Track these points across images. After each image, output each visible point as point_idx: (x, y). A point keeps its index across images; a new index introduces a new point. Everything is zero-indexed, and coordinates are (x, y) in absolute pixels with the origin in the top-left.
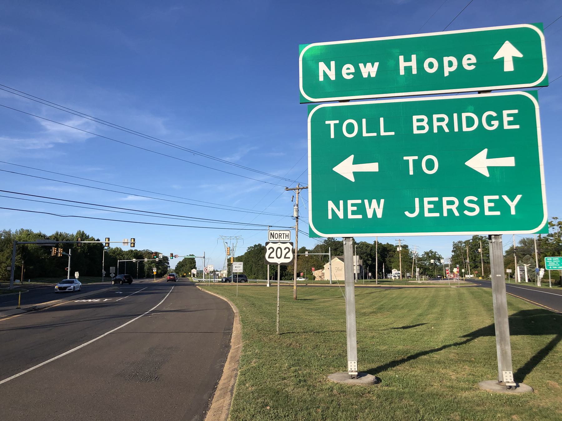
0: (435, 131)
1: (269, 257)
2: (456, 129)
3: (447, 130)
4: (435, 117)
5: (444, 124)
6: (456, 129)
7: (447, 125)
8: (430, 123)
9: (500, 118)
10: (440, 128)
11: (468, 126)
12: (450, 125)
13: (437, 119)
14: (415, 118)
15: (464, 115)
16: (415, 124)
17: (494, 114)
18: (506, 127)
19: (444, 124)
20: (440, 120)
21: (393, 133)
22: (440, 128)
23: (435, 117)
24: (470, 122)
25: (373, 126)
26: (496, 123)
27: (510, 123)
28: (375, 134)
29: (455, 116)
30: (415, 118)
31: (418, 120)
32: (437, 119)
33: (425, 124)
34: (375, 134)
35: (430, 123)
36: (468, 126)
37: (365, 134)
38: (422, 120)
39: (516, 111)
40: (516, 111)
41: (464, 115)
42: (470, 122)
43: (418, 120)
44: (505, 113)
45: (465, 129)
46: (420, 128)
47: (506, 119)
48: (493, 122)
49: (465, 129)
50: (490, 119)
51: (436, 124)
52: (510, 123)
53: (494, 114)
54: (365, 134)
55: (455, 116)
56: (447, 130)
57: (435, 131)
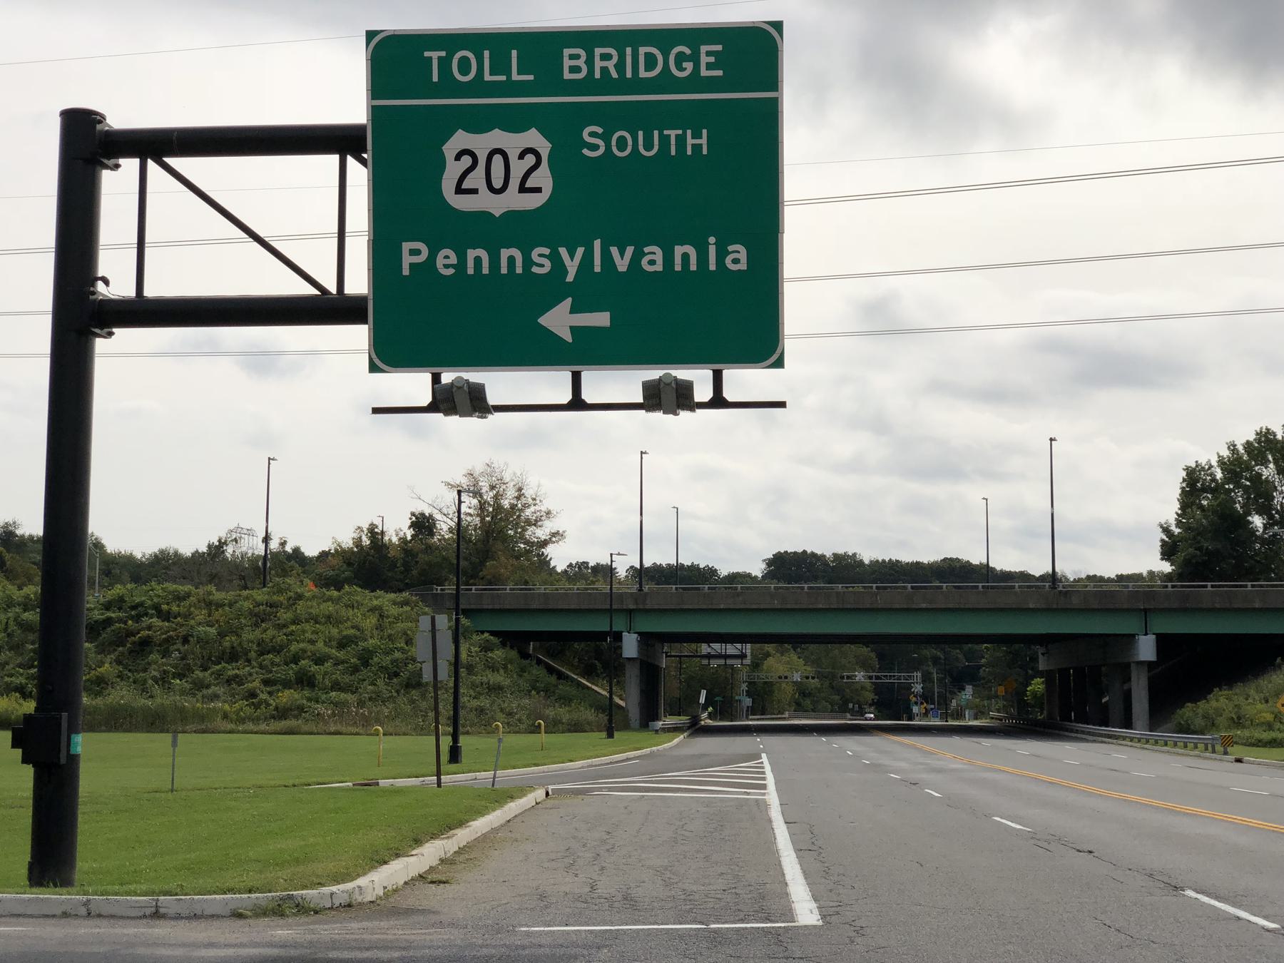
0: (597, 75)
1: (459, 190)
2: (629, 75)
3: (615, 75)
4: (598, 51)
5: (610, 65)
6: (629, 75)
8: (590, 62)
9: (695, 58)
10: (604, 70)
12: (620, 66)
14: (567, 52)
15: (643, 50)
16: (567, 63)
17: (688, 51)
18: (704, 72)
19: (610, 65)
20: (606, 57)
21: (531, 77)
22: (604, 70)
23: (598, 51)
25: (500, 65)
26: (689, 66)
27: (709, 66)
28: (503, 78)
29: (629, 50)
30: (567, 52)
31: (572, 57)
33: (581, 62)
34: (503, 78)
35: (590, 62)
37: (487, 77)
38: (577, 57)
39: (719, 48)
40: (719, 48)
41: (643, 50)
43: (572, 57)
44: (704, 49)
45: (643, 74)
47: (704, 60)
48: (685, 65)
50: (680, 58)
51: (598, 64)
52: (709, 66)
53: (688, 51)
54: (487, 77)
55: (629, 50)
56: (615, 75)
57: (597, 75)
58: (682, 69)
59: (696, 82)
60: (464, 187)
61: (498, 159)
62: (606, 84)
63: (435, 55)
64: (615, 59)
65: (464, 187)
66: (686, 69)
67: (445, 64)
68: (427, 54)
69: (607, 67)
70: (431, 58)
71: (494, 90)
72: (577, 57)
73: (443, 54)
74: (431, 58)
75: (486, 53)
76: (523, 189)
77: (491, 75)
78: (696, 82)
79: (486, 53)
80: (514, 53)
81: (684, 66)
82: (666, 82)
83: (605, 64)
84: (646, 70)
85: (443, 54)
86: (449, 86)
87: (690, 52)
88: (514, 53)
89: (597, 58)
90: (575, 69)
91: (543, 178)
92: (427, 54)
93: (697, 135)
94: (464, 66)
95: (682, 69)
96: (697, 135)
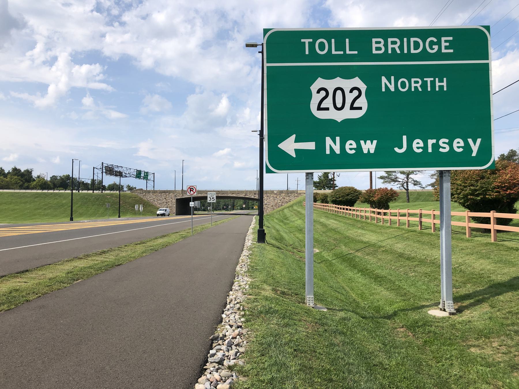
0: (390, 52)
2: (406, 51)
4: (390, 40)
5: (396, 47)
6: (406, 52)
8: (386, 45)
9: (439, 43)
10: (393, 49)
12: (401, 47)
14: (374, 40)
15: (412, 40)
16: (374, 46)
17: (435, 40)
18: (444, 51)
19: (396, 47)
20: (394, 43)
21: (356, 52)
22: (393, 49)
23: (390, 40)
25: (340, 46)
26: (436, 47)
27: (446, 48)
28: (342, 53)
30: (374, 40)
31: (377, 43)
33: (381, 45)
34: (342, 53)
35: (386, 45)
37: (334, 52)
38: (379, 43)
39: (451, 38)
40: (451, 38)
41: (412, 40)
43: (377, 43)
44: (443, 39)
45: (413, 51)
46: (378, 49)
47: (444, 44)
48: (434, 47)
49: (413, 51)
50: (432, 43)
51: (390, 46)
52: (446, 48)
53: (435, 40)
54: (334, 52)
57: (390, 52)
58: (432, 49)
59: (439, 55)
61: (339, 93)
62: (394, 56)
63: (307, 41)
64: (399, 44)
66: (434, 49)
67: (312, 45)
68: (303, 40)
70: (305, 43)
72: (379, 43)
73: (311, 40)
74: (305, 43)
75: (333, 40)
76: (352, 108)
78: (439, 55)
79: (333, 40)
80: (347, 40)
82: (424, 55)
83: (393, 46)
84: (414, 49)
85: (311, 40)
86: (314, 56)
87: (437, 41)
88: (347, 40)
89: (389, 43)
90: (378, 49)
91: (362, 102)
92: (303, 40)
94: (322, 46)
95: (432, 49)
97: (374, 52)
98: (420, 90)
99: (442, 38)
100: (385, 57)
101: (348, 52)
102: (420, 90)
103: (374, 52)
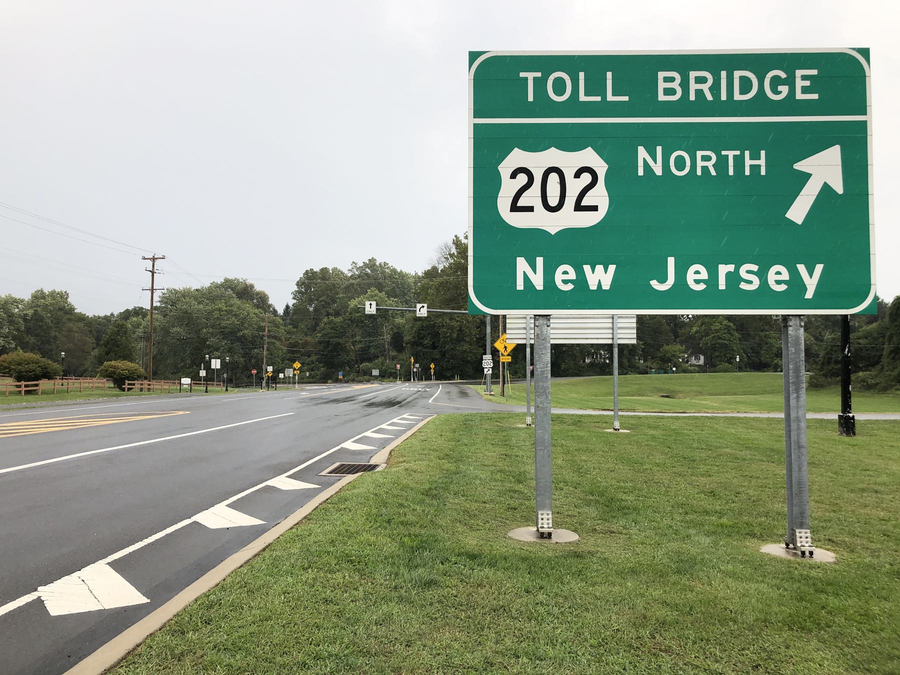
0: (692, 97)
1: (515, 208)
2: (724, 97)
3: (709, 97)
4: (693, 75)
5: (705, 87)
6: (724, 97)
7: (709, 88)
8: (685, 85)
9: (790, 82)
10: (699, 93)
11: (743, 92)
12: (715, 89)
13: (696, 78)
14: (661, 75)
15: (737, 74)
16: (662, 85)
17: (783, 75)
18: (799, 96)
19: (705, 87)
20: (700, 80)
21: (626, 98)
22: (699, 93)
23: (693, 75)
24: (746, 85)
27: (805, 90)
28: (598, 99)
29: (724, 74)
30: (661, 75)
31: (667, 80)
32: (696, 78)
33: (676, 85)
34: (598, 99)
35: (685, 85)
36: (743, 92)
37: (583, 98)
38: (672, 80)
39: (814, 72)
40: (814, 72)
41: (737, 74)
42: (746, 85)
43: (667, 80)
44: (799, 73)
45: (737, 97)
46: (671, 92)
47: (800, 84)
48: (780, 88)
49: (737, 97)
50: (776, 82)
51: (693, 87)
52: (805, 90)
53: (783, 75)
54: (583, 98)
55: (724, 74)
56: (709, 97)
57: (692, 97)
60: (583, 203)
61: (554, 178)
62: (701, 106)
63: (530, 76)
65: (583, 203)
67: (540, 84)
68: (522, 75)
69: (702, 90)
70: (526, 79)
71: (717, 108)
72: (672, 80)
73: (539, 75)
74: (526, 79)
75: (582, 75)
77: (613, 95)
78: (791, 106)
79: (582, 75)
80: (609, 75)
81: (779, 90)
82: (761, 105)
83: (700, 86)
85: (539, 75)
86: (544, 106)
87: (786, 76)
90: (669, 92)
92: (522, 75)
93: (755, 156)
94: (559, 87)
96: (755, 156)
97: (662, 97)
98: (713, 173)
99: (797, 71)
100: (683, 107)
101: (610, 97)
102: (713, 173)
103: (662, 97)
